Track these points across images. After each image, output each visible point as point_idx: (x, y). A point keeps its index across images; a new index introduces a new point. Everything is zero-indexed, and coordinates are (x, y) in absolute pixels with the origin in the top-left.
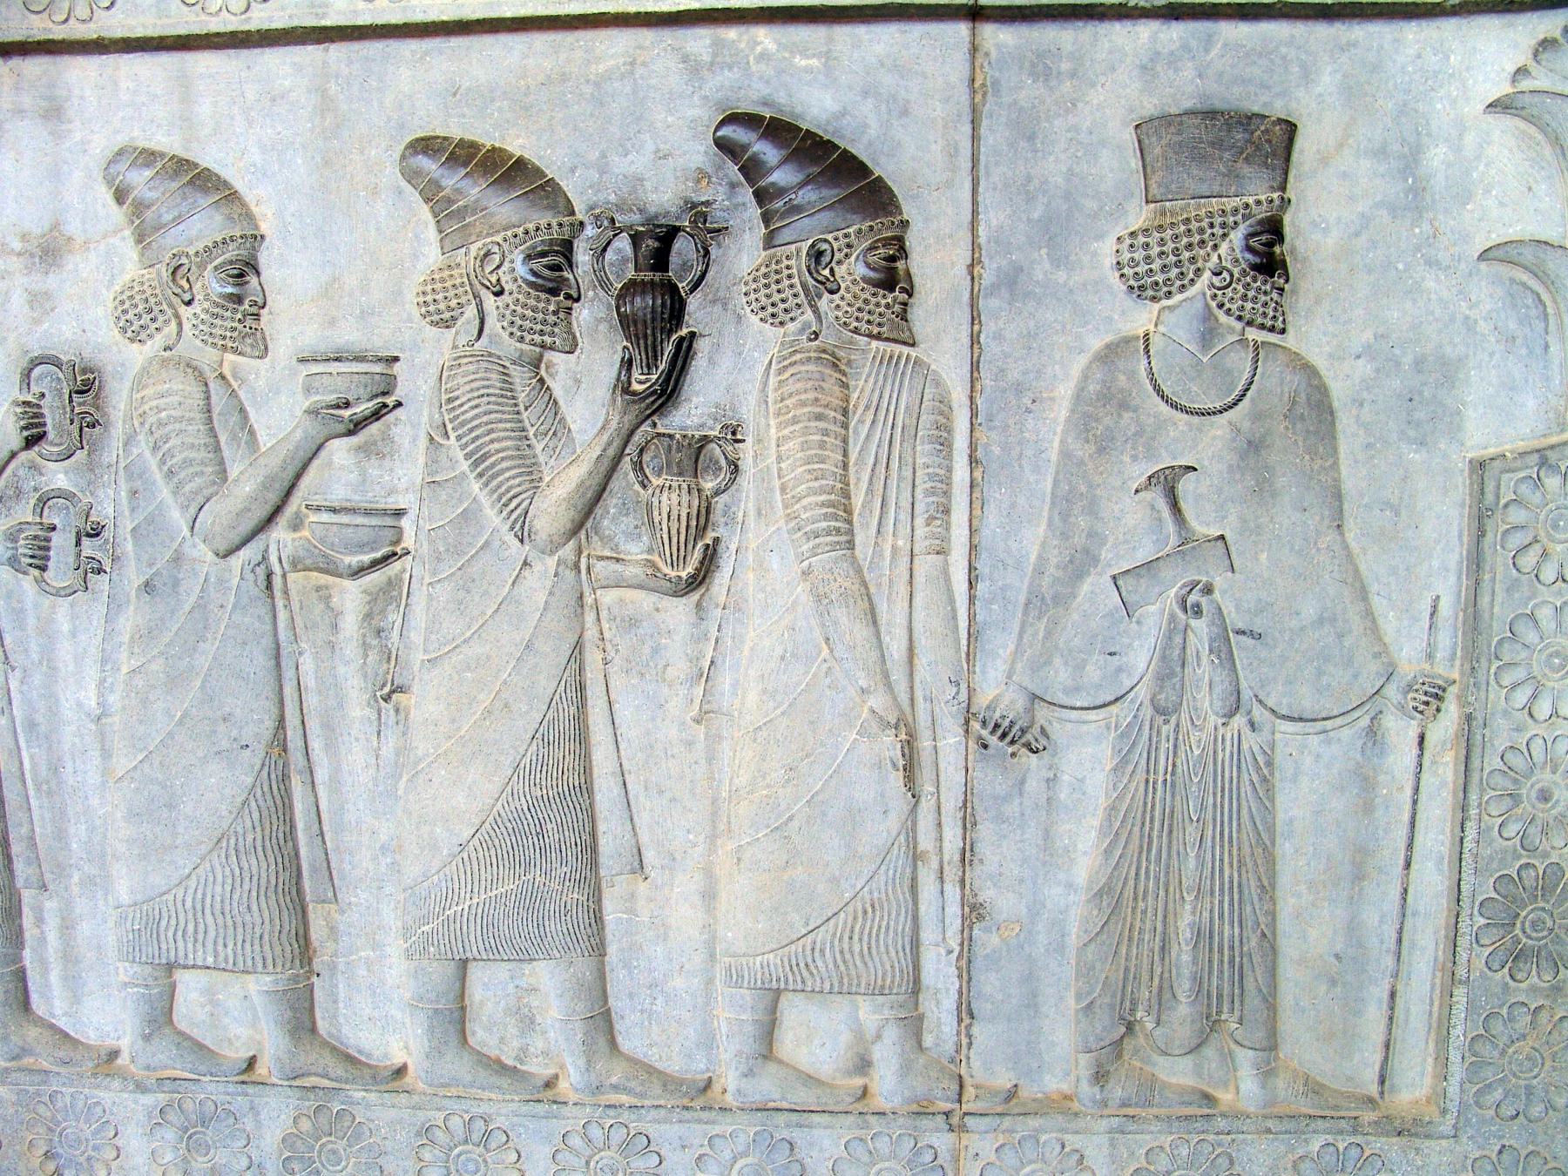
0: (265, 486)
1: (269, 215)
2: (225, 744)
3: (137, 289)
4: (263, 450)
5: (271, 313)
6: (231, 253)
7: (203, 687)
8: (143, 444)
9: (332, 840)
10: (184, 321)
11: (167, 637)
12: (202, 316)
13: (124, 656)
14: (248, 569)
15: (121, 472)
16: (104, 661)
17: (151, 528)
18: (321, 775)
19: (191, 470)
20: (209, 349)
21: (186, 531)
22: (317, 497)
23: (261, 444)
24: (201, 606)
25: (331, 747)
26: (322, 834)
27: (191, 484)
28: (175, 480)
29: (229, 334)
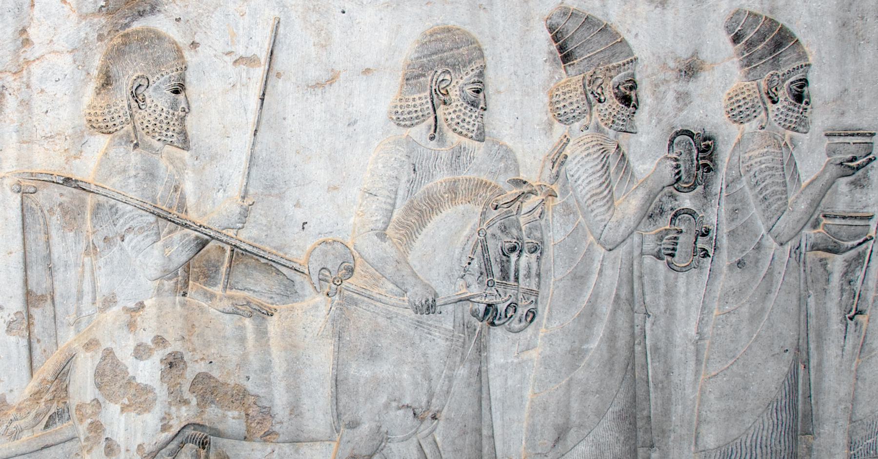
0: (811, 205)
1: (814, 53)
2: (777, 350)
3: (747, 93)
4: (803, 184)
5: (812, 108)
7: (769, 319)
8: (745, 183)
9: (814, 399)
10: (770, 111)
11: (751, 292)
12: (782, 110)
13: (716, 305)
14: (793, 251)
15: (723, 199)
16: (703, 308)
17: (745, 231)
18: (813, 362)
19: (776, 197)
20: (780, 128)
21: (764, 232)
22: (828, 210)
23: (802, 181)
24: (770, 273)
25: (819, 348)
26: (810, 396)
27: (776, 205)
28: (767, 203)
29: (794, 120)
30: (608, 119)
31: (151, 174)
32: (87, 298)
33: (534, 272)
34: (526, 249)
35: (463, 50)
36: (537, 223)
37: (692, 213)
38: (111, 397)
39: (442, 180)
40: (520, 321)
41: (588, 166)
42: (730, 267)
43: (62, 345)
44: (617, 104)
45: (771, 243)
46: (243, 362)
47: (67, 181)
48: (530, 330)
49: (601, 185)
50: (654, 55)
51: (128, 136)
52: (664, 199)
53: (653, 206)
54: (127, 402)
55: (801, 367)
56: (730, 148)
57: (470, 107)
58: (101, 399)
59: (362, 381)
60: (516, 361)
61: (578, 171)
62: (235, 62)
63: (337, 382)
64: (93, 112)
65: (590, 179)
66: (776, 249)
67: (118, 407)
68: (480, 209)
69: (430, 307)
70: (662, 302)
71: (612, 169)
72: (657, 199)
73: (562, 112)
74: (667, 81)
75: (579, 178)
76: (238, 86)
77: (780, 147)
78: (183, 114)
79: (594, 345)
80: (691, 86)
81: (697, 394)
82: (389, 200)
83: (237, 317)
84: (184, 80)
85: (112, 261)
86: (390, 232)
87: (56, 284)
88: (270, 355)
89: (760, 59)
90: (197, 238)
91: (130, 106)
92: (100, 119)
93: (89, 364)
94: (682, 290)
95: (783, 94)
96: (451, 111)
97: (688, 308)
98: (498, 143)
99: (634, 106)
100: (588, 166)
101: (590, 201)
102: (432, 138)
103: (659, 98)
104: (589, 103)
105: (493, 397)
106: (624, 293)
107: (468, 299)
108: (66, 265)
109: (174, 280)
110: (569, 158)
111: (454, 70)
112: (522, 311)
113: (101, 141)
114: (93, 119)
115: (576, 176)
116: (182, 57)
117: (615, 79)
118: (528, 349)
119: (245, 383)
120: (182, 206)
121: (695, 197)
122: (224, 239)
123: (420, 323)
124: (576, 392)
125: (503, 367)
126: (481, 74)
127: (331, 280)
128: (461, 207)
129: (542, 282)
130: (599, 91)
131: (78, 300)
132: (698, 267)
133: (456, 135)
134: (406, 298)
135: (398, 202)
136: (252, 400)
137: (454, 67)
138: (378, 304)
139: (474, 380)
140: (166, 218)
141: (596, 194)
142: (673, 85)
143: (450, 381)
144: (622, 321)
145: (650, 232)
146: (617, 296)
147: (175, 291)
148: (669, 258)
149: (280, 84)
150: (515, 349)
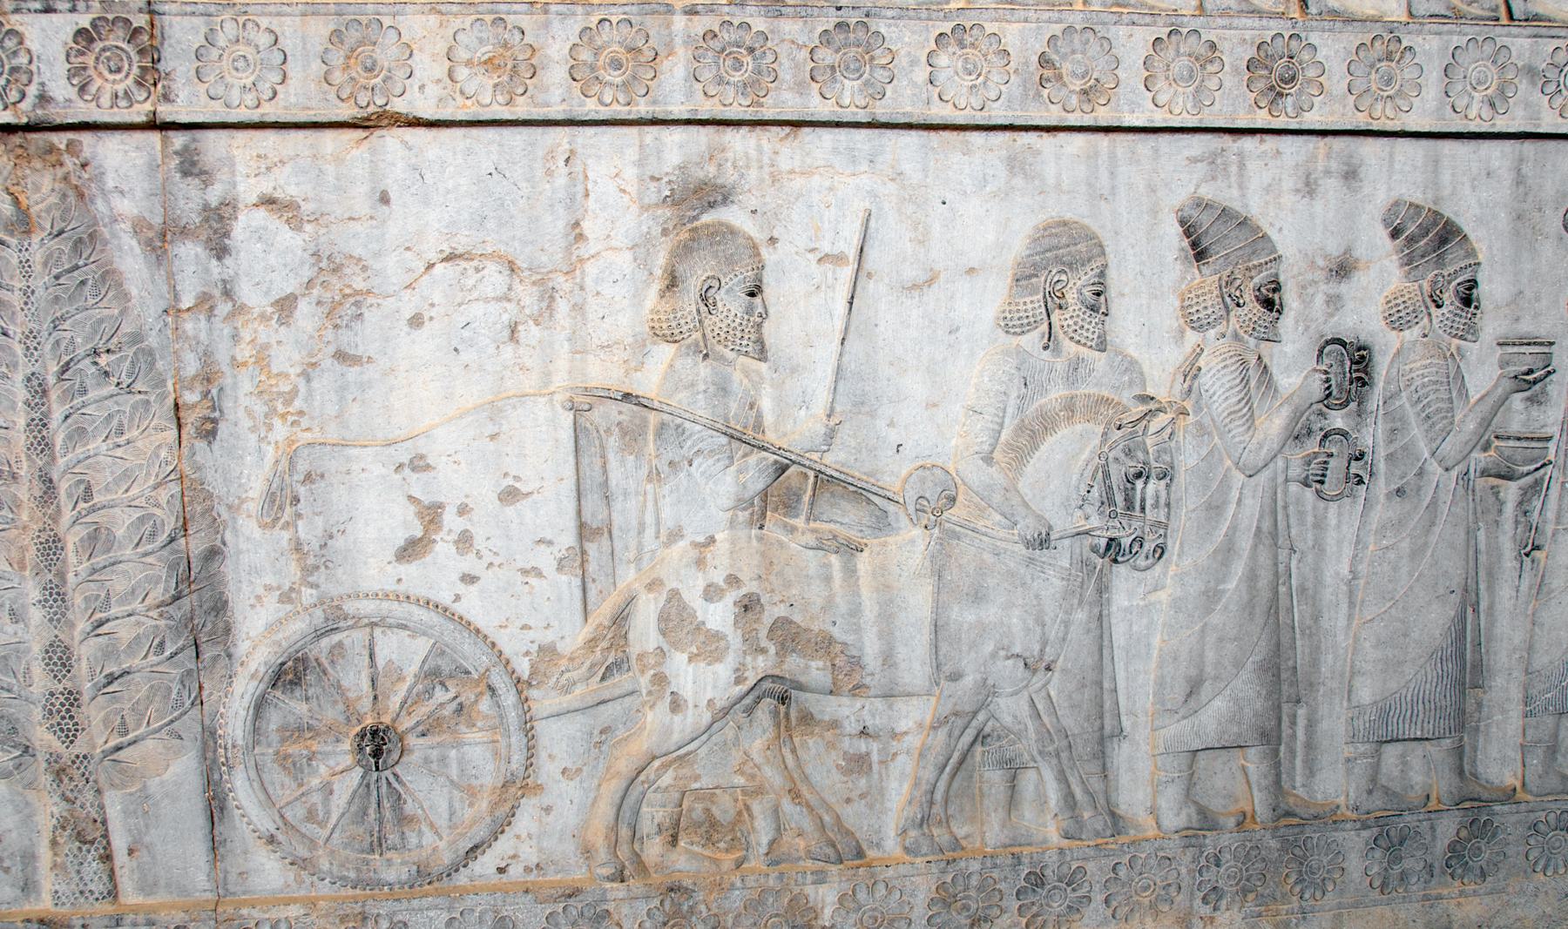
2: (1441, 591)
3: (1407, 296)
4: (1472, 401)
6: (1467, 276)
7: (1432, 555)
8: (1405, 399)
11: (1412, 524)
13: (1372, 539)
15: (1380, 417)
16: (1358, 542)
21: (1426, 455)
24: (1434, 503)
30: (1248, 326)
31: (723, 389)
32: (650, 532)
33: (1162, 501)
34: (1153, 475)
35: (1082, 247)
36: (1166, 445)
37: (1344, 434)
38: (676, 645)
39: (1057, 395)
40: (1147, 557)
41: (1225, 380)
42: (1388, 496)
43: (621, 585)
44: (1258, 309)
45: (1434, 468)
46: (829, 604)
47: (627, 396)
48: (1158, 568)
49: (1240, 401)
50: (1300, 252)
51: (697, 345)
52: (1312, 418)
53: (1299, 425)
54: (695, 651)
55: (1470, 610)
56: (1388, 359)
57: (1089, 312)
58: (666, 647)
59: (966, 626)
60: (1142, 603)
61: (1213, 385)
62: (820, 260)
63: (936, 628)
64: (656, 317)
65: (1227, 394)
66: (1441, 475)
67: (685, 656)
68: (1100, 429)
69: (1043, 542)
70: (1310, 536)
71: (1253, 383)
72: (1304, 418)
73: (1195, 318)
74: (1316, 282)
75: (1214, 393)
76: (823, 287)
77: (1445, 357)
78: (759, 320)
79: (1231, 585)
80: (1344, 288)
81: (1351, 641)
82: (996, 419)
83: (822, 553)
84: (761, 281)
85: (678, 489)
86: (997, 455)
87: (615, 516)
88: (860, 596)
89: (1423, 256)
90: (776, 462)
91: (698, 311)
92: (665, 326)
93: (652, 607)
94: (1333, 522)
95: (1448, 297)
96: (1067, 316)
97: (1339, 542)
98: (1121, 353)
99: (1278, 311)
100: (1225, 380)
101: (1228, 420)
102: (1046, 348)
103: (1307, 302)
104: (1226, 307)
105: (1115, 645)
106: (1267, 525)
107: (1087, 533)
108: (625, 494)
109: (750, 511)
110: (1203, 371)
111: (1071, 269)
112: (1149, 546)
113: (667, 351)
114: (657, 325)
115: (1211, 392)
116: (759, 254)
117: (1257, 280)
118: (1155, 590)
119: (831, 629)
120: (759, 426)
121: (1348, 415)
122: (807, 463)
123: (1031, 561)
124: (1211, 639)
125: (1128, 610)
126: (1102, 274)
127: (929, 510)
128: (1079, 427)
129: (1172, 513)
130: (1238, 294)
131: (639, 533)
132: (1352, 495)
133: (1073, 344)
134: (1016, 532)
135: (1007, 421)
136: (838, 648)
137: (1071, 266)
138: (984, 538)
139: (1093, 625)
140: (740, 440)
141: (1235, 412)
142: (1323, 287)
143: (1066, 627)
144: (1264, 558)
145: (1297, 455)
146: (1259, 529)
147: (751, 523)
148: (1318, 486)
149: (871, 284)
150: (1141, 590)
